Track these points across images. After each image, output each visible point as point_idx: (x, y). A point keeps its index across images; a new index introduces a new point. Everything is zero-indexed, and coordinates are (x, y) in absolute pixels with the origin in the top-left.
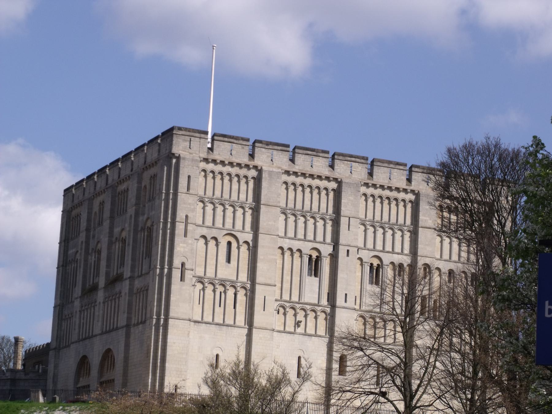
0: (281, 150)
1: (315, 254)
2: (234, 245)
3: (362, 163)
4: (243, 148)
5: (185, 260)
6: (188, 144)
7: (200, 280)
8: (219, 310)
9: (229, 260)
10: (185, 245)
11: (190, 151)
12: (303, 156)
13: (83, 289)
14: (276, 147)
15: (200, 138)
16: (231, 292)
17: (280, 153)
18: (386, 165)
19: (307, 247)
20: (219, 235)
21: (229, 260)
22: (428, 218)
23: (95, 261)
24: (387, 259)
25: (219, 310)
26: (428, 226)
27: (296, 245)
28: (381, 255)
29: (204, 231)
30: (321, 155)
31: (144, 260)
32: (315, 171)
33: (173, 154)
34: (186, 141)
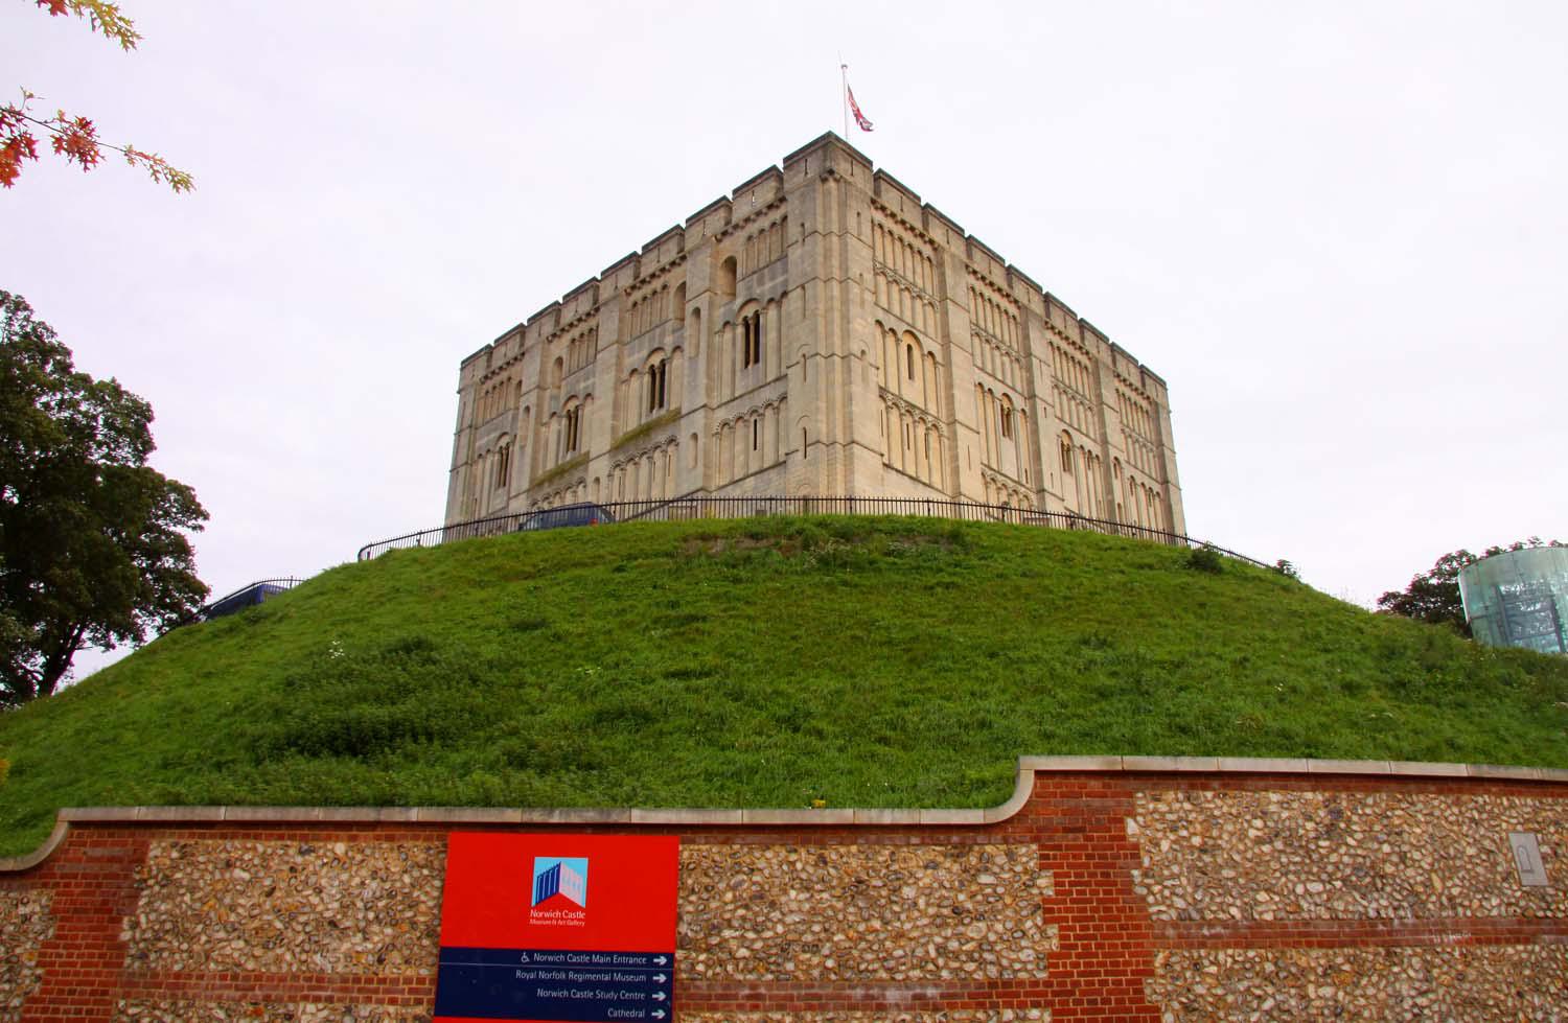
1: (1006, 405)
2: (916, 353)
5: (866, 350)
7: (883, 393)
8: (909, 455)
9: (911, 376)
10: (864, 323)
13: (532, 481)
16: (921, 430)
19: (999, 389)
20: (901, 328)
21: (911, 376)
23: (559, 432)
24: (1078, 439)
25: (909, 455)
27: (988, 382)
28: (1070, 430)
29: (881, 316)
31: (738, 374)
33: (831, 172)
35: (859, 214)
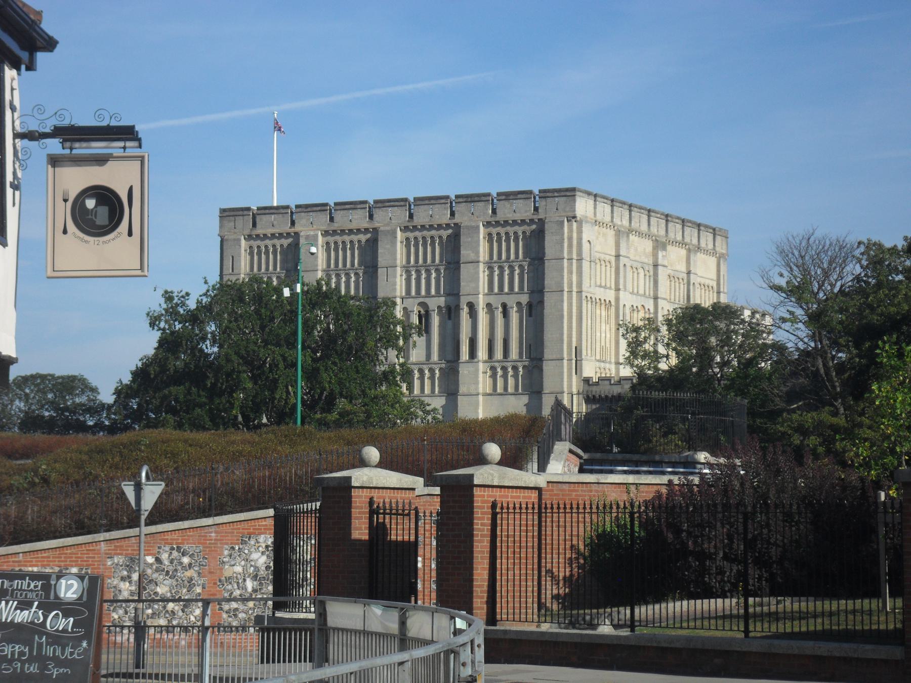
0: (320, 211)
3: (401, 206)
4: (283, 217)
6: (232, 224)
11: (235, 230)
12: (342, 212)
14: (315, 209)
15: (243, 215)
17: (319, 213)
18: (427, 202)
22: (470, 252)
26: (470, 260)
28: (427, 300)
30: (359, 206)
32: (354, 226)
34: (230, 221)
35: (233, 257)
